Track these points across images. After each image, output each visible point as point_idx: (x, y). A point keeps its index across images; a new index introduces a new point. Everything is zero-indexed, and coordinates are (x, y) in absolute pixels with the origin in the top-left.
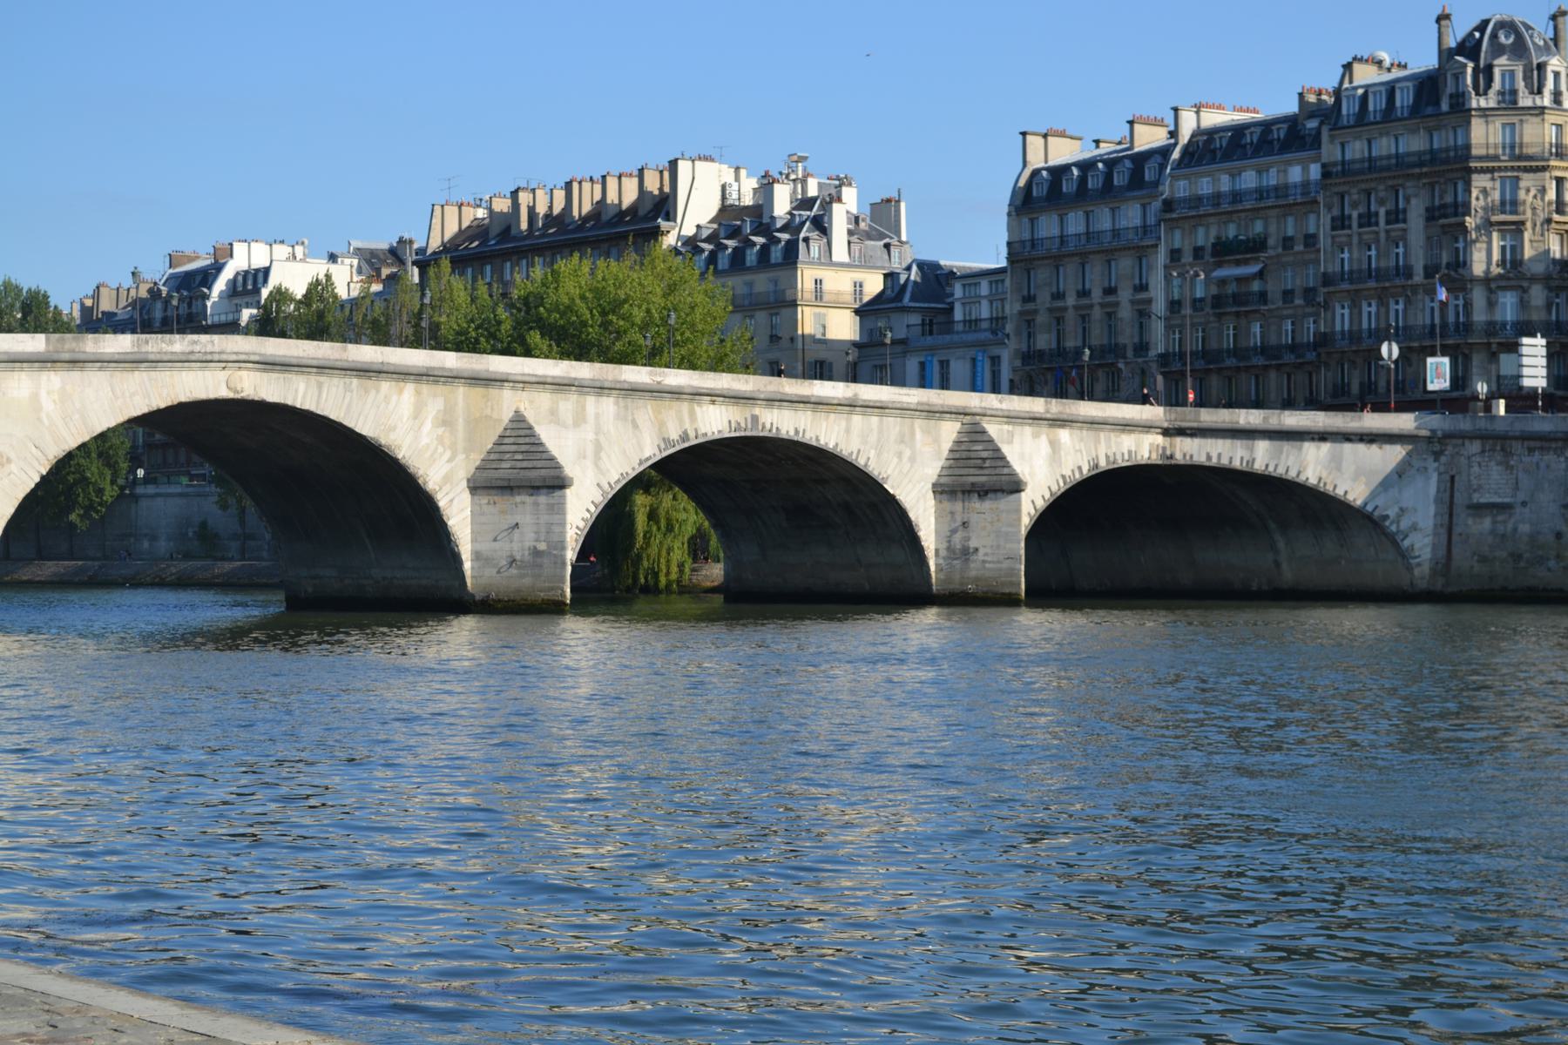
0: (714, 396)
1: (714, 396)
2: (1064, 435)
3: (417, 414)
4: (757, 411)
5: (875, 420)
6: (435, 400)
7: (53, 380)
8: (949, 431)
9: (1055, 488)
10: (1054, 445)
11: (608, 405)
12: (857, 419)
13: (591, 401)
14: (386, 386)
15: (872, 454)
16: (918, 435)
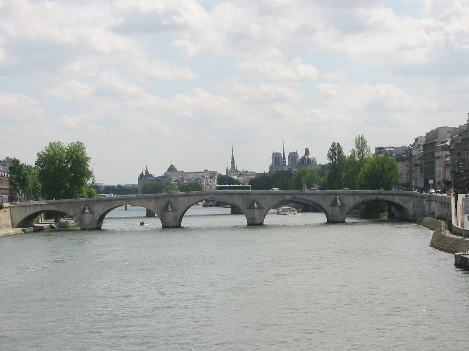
0: (287, 194)
1: (287, 194)
2: (356, 196)
3: (239, 199)
4: (296, 196)
5: (318, 196)
6: (241, 198)
7: (186, 198)
8: (333, 197)
9: (354, 204)
10: (354, 198)
11: (270, 197)
12: (315, 196)
13: (267, 196)
14: (234, 196)
15: (318, 201)
16: (327, 198)
